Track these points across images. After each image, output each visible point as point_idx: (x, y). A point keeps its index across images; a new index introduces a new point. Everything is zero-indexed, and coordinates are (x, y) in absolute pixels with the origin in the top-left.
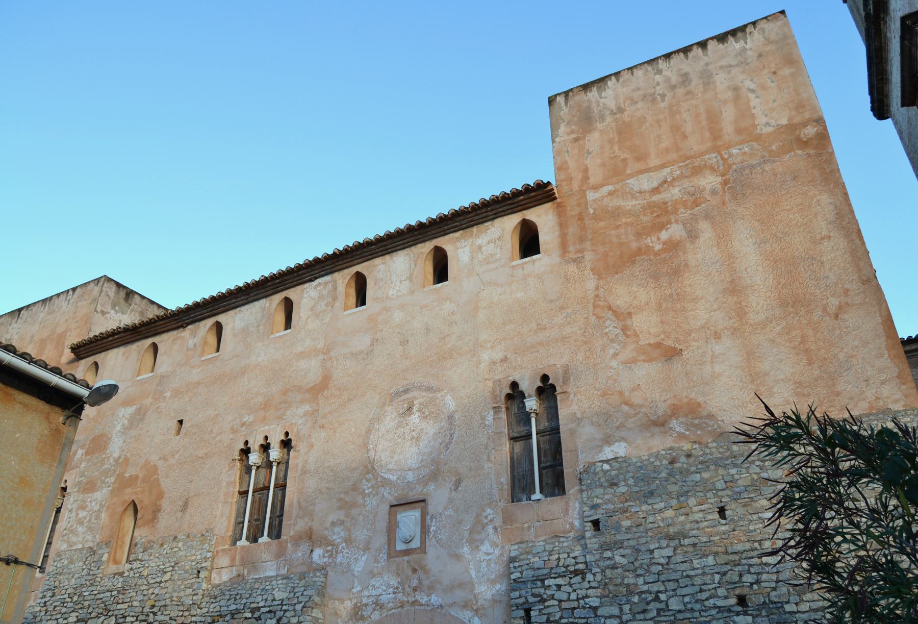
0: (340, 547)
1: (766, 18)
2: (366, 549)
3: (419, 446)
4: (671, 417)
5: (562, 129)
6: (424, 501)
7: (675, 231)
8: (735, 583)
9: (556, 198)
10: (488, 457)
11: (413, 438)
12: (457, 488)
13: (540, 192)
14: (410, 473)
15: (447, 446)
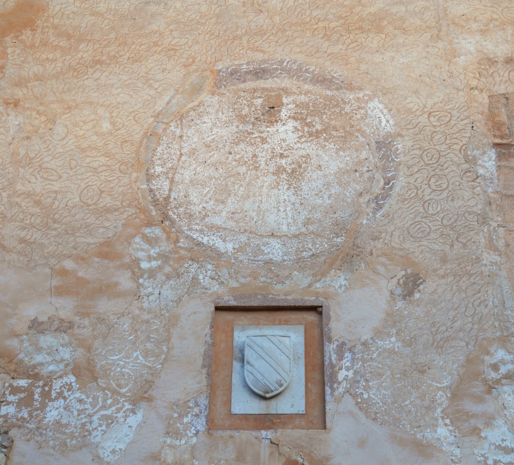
0: (57, 385)
2: (142, 396)
3: (297, 190)
6: (315, 309)
10: (491, 240)
11: (279, 171)
12: (411, 293)
14: (275, 243)
15: (378, 202)
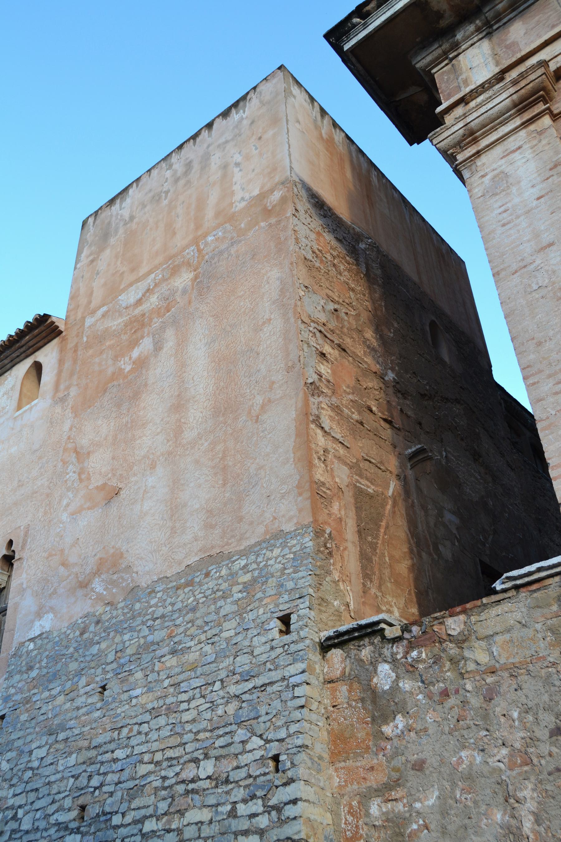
1: (265, 79)
4: (95, 574)
5: (86, 252)
7: (147, 344)
8: (82, 789)
9: (61, 332)
13: (42, 328)
